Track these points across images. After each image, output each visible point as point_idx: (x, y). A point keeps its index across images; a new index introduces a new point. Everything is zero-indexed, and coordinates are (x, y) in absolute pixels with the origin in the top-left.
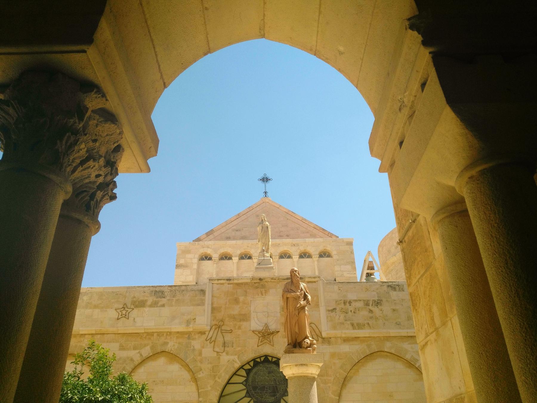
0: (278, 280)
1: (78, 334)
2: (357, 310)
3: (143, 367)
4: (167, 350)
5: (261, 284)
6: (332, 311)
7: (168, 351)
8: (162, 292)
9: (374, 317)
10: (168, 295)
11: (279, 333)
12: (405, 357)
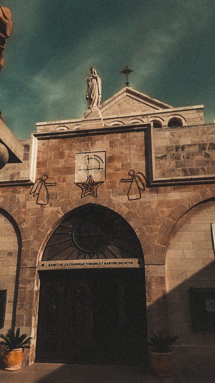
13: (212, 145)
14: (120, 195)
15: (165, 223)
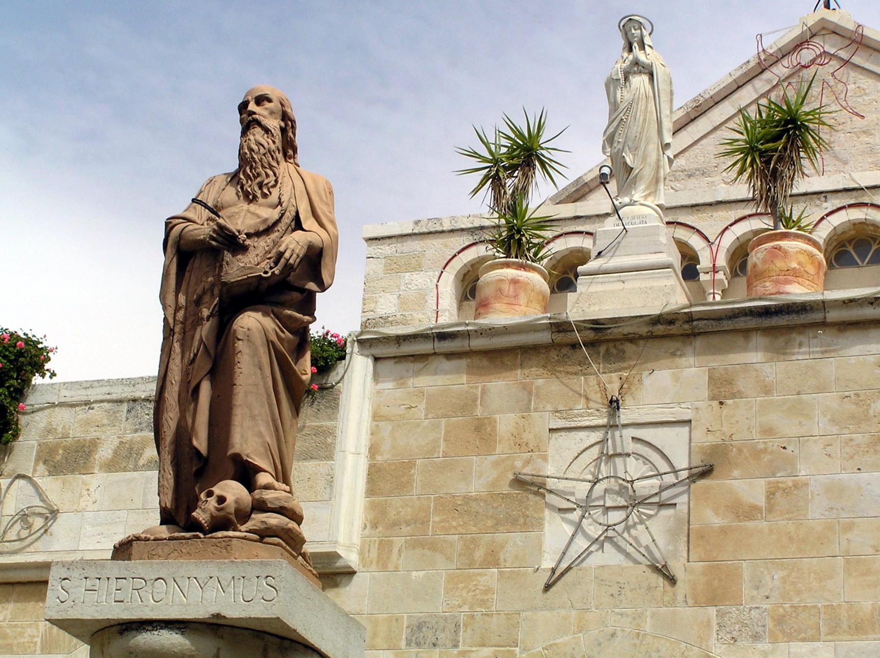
0: (686, 326)
14: (756, 637)
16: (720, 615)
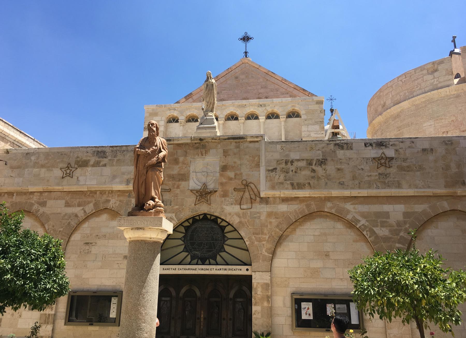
0: (219, 140)
1: (28, 192)
2: (299, 169)
3: (87, 223)
4: (108, 208)
5: (202, 144)
6: (272, 171)
7: (110, 208)
8: (104, 152)
9: (316, 177)
10: (109, 155)
11: (217, 194)
12: (346, 218)
13: (319, 161)
14: (232, 204)
15: (272, 233)
16: (225, 200)
